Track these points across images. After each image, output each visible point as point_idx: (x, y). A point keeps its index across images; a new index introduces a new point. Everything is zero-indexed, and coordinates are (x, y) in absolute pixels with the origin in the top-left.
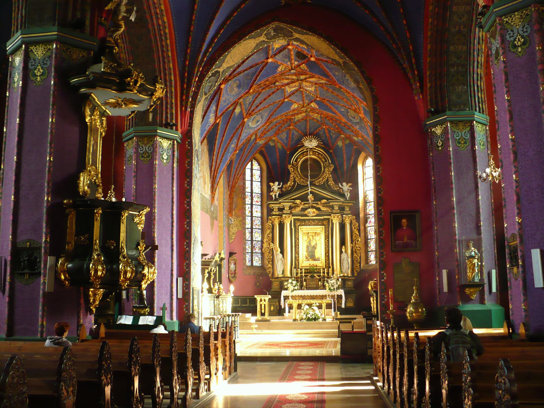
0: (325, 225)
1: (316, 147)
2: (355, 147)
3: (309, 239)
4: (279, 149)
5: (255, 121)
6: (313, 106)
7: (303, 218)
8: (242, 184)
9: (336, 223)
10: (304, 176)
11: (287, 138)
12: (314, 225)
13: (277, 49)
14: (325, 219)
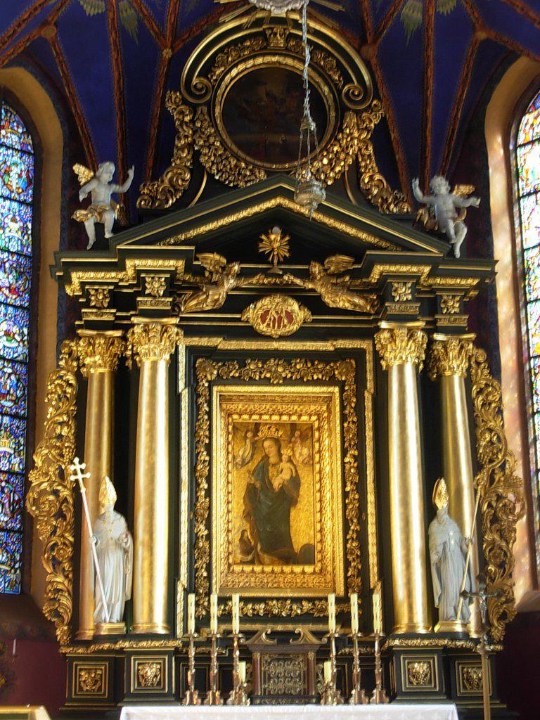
0: (342, 385)
2: (482, 35)
3: (258, 458)
4: (122, 31)
7: (233, 345)
9: (401, 369)
10: (240, 146)
12: (287, 382)
14: (340, 355)
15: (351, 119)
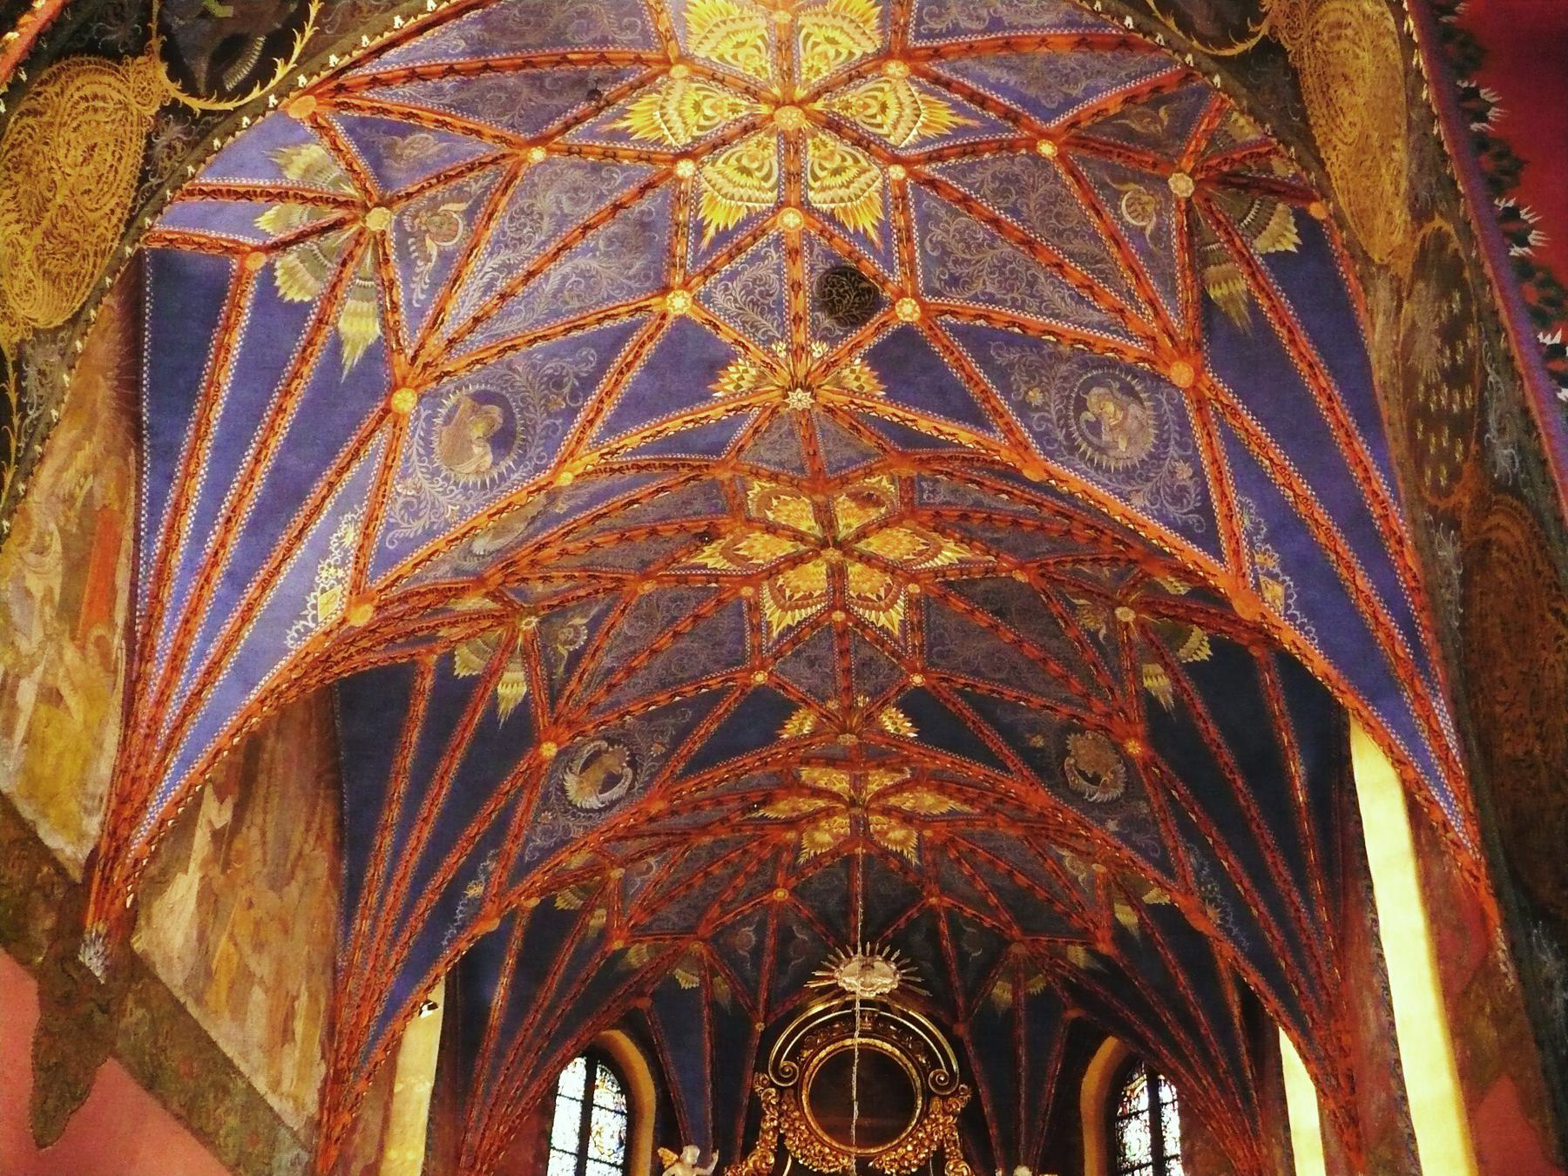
1: (891, 994)
2: (1072, 1014)
4: (714, 1005)
5: (597, 774)
6: (890, 728)
8: (529, 1156)
11: (757, 952)
13: (723, 236)
15: (936, 1104)
